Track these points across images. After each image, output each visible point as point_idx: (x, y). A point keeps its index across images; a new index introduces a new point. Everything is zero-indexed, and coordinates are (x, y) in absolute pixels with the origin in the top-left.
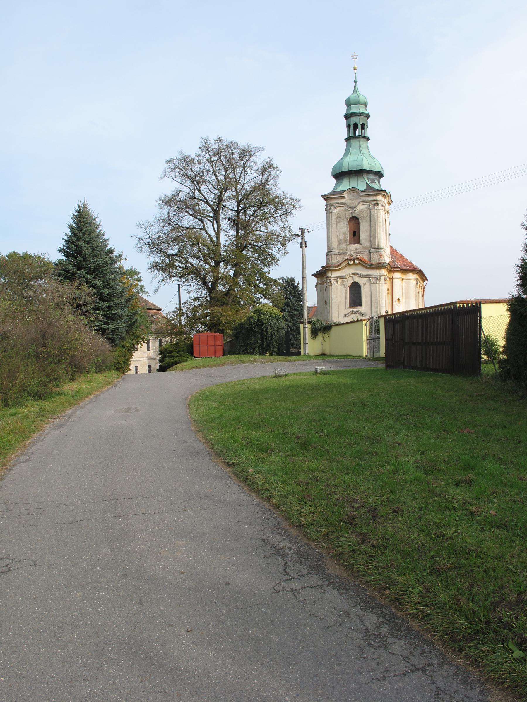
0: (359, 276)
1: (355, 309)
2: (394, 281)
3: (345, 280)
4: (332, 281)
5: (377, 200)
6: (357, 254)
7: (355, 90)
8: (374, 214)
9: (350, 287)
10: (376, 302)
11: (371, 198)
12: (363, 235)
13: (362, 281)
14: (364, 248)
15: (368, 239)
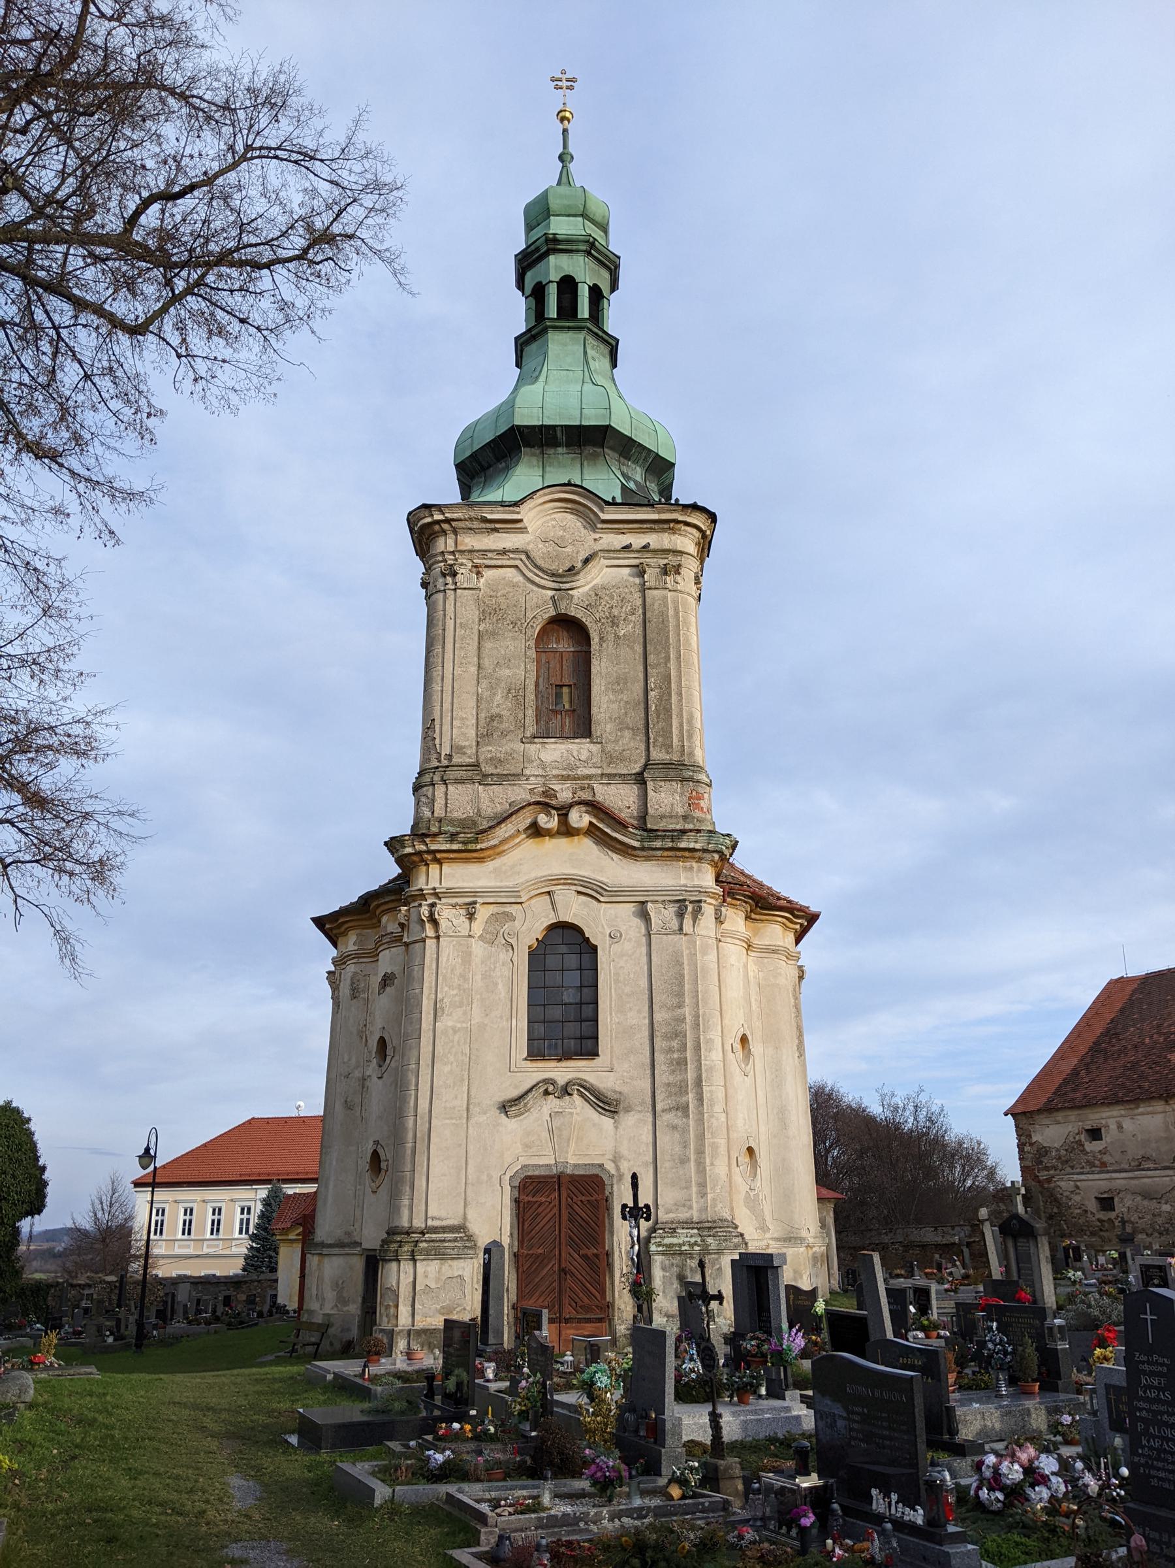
0: (593, 891)
1: (562, 1072)
4: (448, 916)
7: (564, 178)
8: (663, 615)
9: (532, 954)
10: (678, 1034)
11: (654, 540)
12: (605, 704)
13: (599, 922)
14: (610, 759)
15: (637, 717)
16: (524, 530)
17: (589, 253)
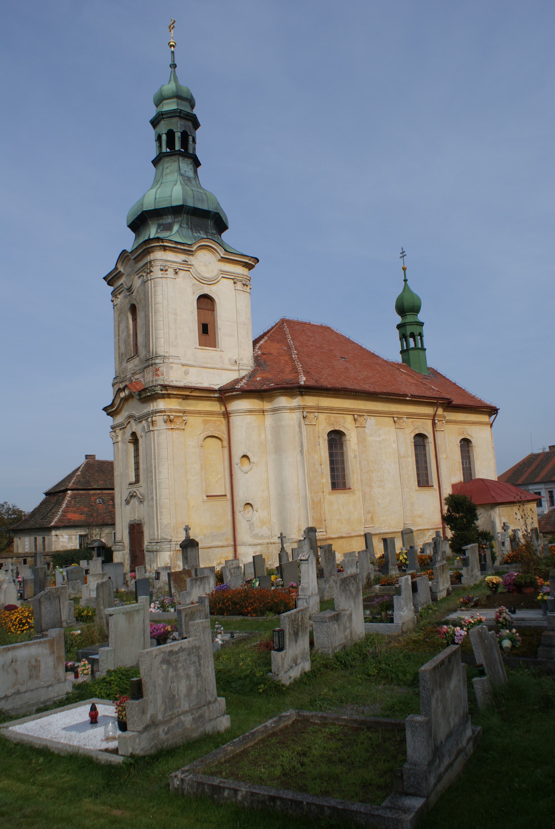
2: (235, 420)
3: (126, 430)
5: (150, 262)
6: (136, 377)
16: (123, 274)
17: (163, 118)
